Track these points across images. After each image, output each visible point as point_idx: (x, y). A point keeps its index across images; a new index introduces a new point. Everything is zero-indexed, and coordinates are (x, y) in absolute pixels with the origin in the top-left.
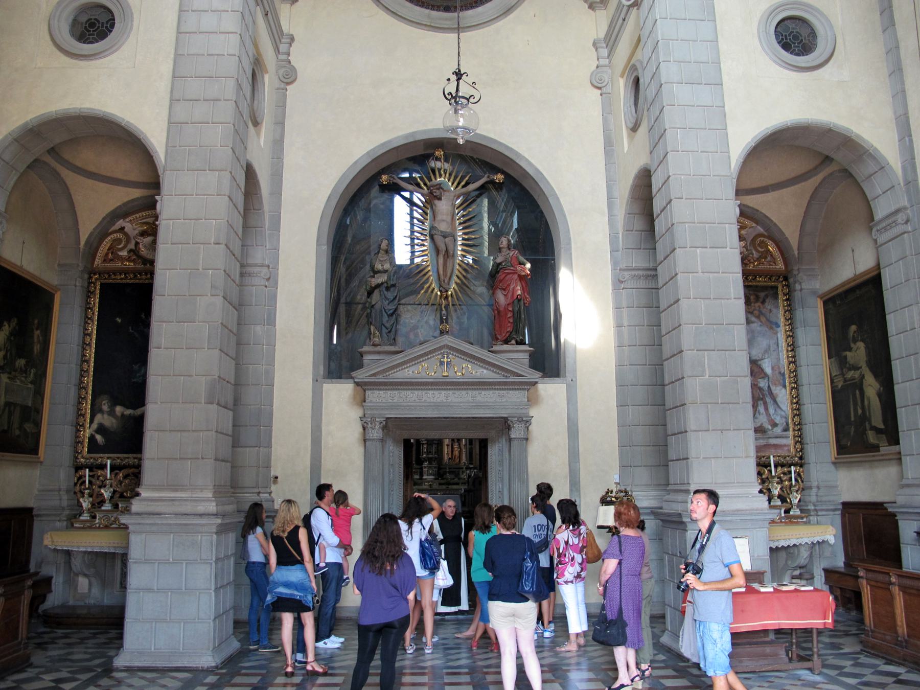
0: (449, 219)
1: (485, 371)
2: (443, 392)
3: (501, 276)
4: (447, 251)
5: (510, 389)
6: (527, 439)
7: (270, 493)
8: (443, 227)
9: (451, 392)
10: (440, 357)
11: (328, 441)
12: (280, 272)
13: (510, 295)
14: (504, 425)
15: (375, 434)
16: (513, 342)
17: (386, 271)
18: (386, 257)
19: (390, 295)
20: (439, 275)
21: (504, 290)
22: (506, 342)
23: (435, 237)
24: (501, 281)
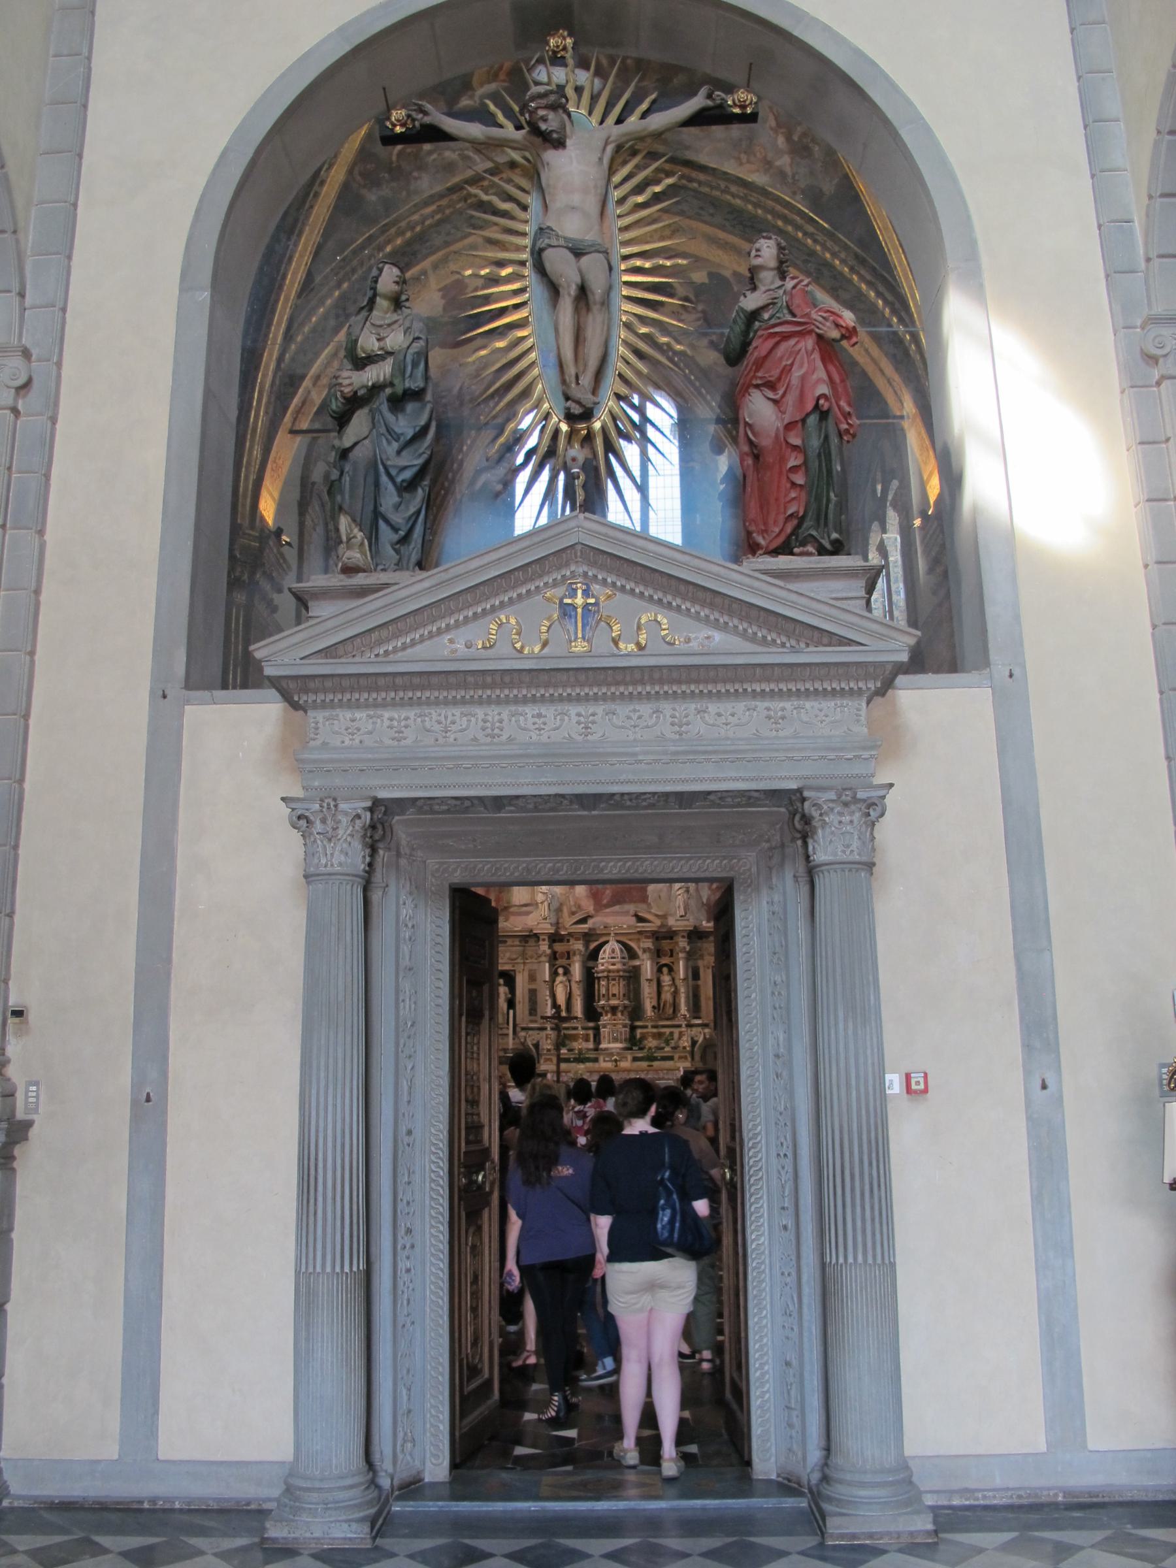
0: (593, 207)
1: (718, 636)
2: (573, 710)
3: (760, 346)
4: (583, 291)
5: (807, 694)
6: (870, 866)
9: (600, 709)
10: (560, 591)
11: (193, 890)
12: (68, 370)
13: (791, 399)
14: (790, 818)
15: (338, 858)
18: (391, 317)
19: (405, 425)
20: (561, 366)
21: (772, 386)
23: (548, 255)
24: (760, 363)
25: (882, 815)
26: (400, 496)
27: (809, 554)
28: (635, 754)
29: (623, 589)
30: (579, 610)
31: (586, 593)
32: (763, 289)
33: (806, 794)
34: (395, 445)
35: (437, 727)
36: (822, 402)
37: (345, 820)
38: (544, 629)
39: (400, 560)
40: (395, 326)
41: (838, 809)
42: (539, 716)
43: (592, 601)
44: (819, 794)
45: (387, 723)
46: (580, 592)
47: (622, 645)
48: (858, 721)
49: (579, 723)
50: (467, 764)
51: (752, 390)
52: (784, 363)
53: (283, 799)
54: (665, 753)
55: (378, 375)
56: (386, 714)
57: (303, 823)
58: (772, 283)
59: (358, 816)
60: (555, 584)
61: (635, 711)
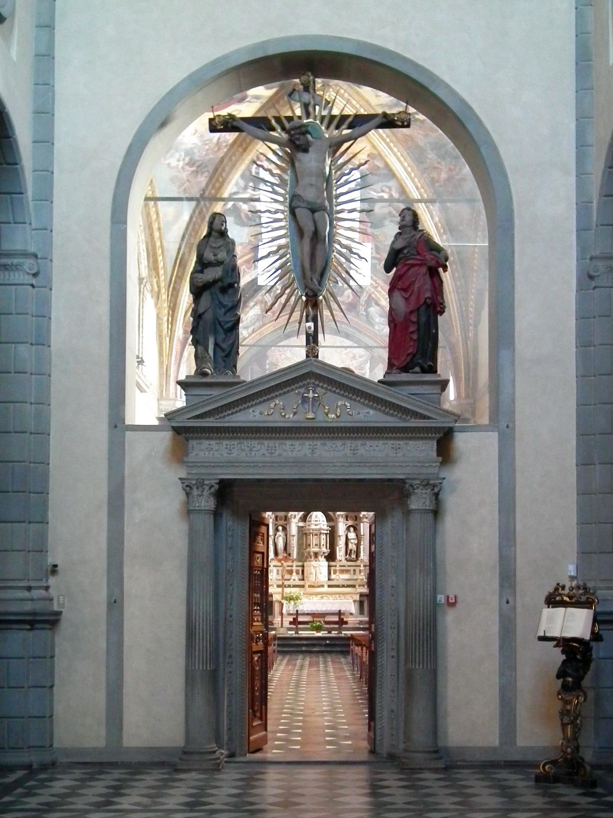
1: (372, 412)
2: (307, 443)
5: (410, 439)
7: (47, 588)
8: (309, 195)
10: (302, 390)
13: (413, 298)
16: (417, 369)
17: (219, 263)
22: (405, 369)
25: (440, 490)
26: (226, 334)
27: (417, 373)
28: (333, 463)
29: (330, 390)
30: (311, 399)
31: (314, 392)
32: (406, 236)
33: (407, 481)
34: (223, 310)
35: (247, 449)
36: (427, 300)
37: (207, 488)
38: (295, 407)
39: (225, 366)
40: (222, 247)
41: (421, 487)
42: (292, 445)
43: (316, 395)
44: (413, 481)
45: (225, 446)
46: (311, 391)
47: (329, 415)
48: (432, 450)
49: (309, 449)
50: (260, 465)
51: (395, 290)
52: (411, 280)
53: (180, 479)
54: (347, 462)
55: (215, 276)
56: (225, 442)
57: (188, 489)
58: (410, 233)
59: (212, 486)
60: (300, 387)
61: (334, 444)
